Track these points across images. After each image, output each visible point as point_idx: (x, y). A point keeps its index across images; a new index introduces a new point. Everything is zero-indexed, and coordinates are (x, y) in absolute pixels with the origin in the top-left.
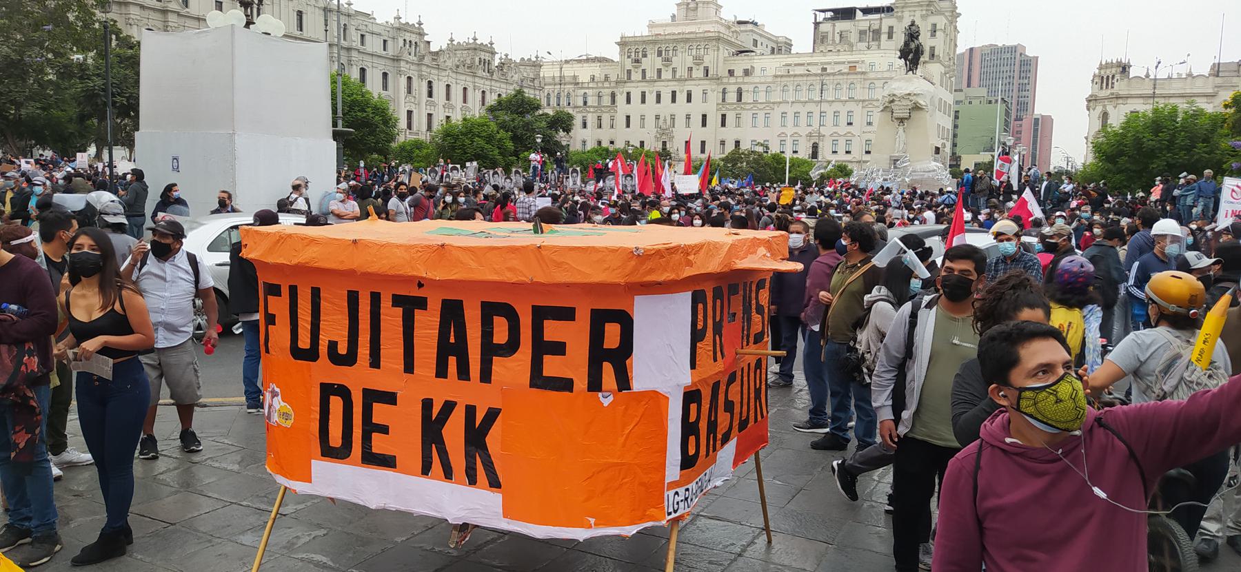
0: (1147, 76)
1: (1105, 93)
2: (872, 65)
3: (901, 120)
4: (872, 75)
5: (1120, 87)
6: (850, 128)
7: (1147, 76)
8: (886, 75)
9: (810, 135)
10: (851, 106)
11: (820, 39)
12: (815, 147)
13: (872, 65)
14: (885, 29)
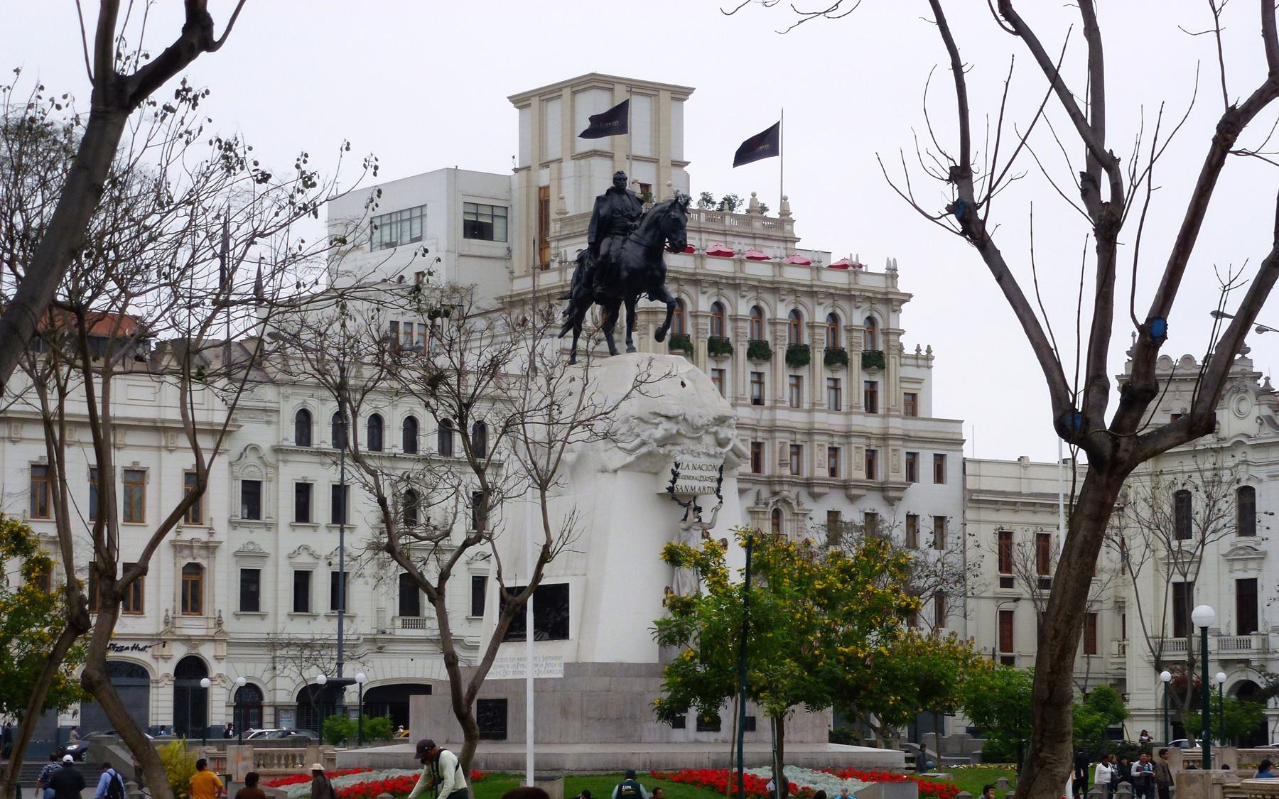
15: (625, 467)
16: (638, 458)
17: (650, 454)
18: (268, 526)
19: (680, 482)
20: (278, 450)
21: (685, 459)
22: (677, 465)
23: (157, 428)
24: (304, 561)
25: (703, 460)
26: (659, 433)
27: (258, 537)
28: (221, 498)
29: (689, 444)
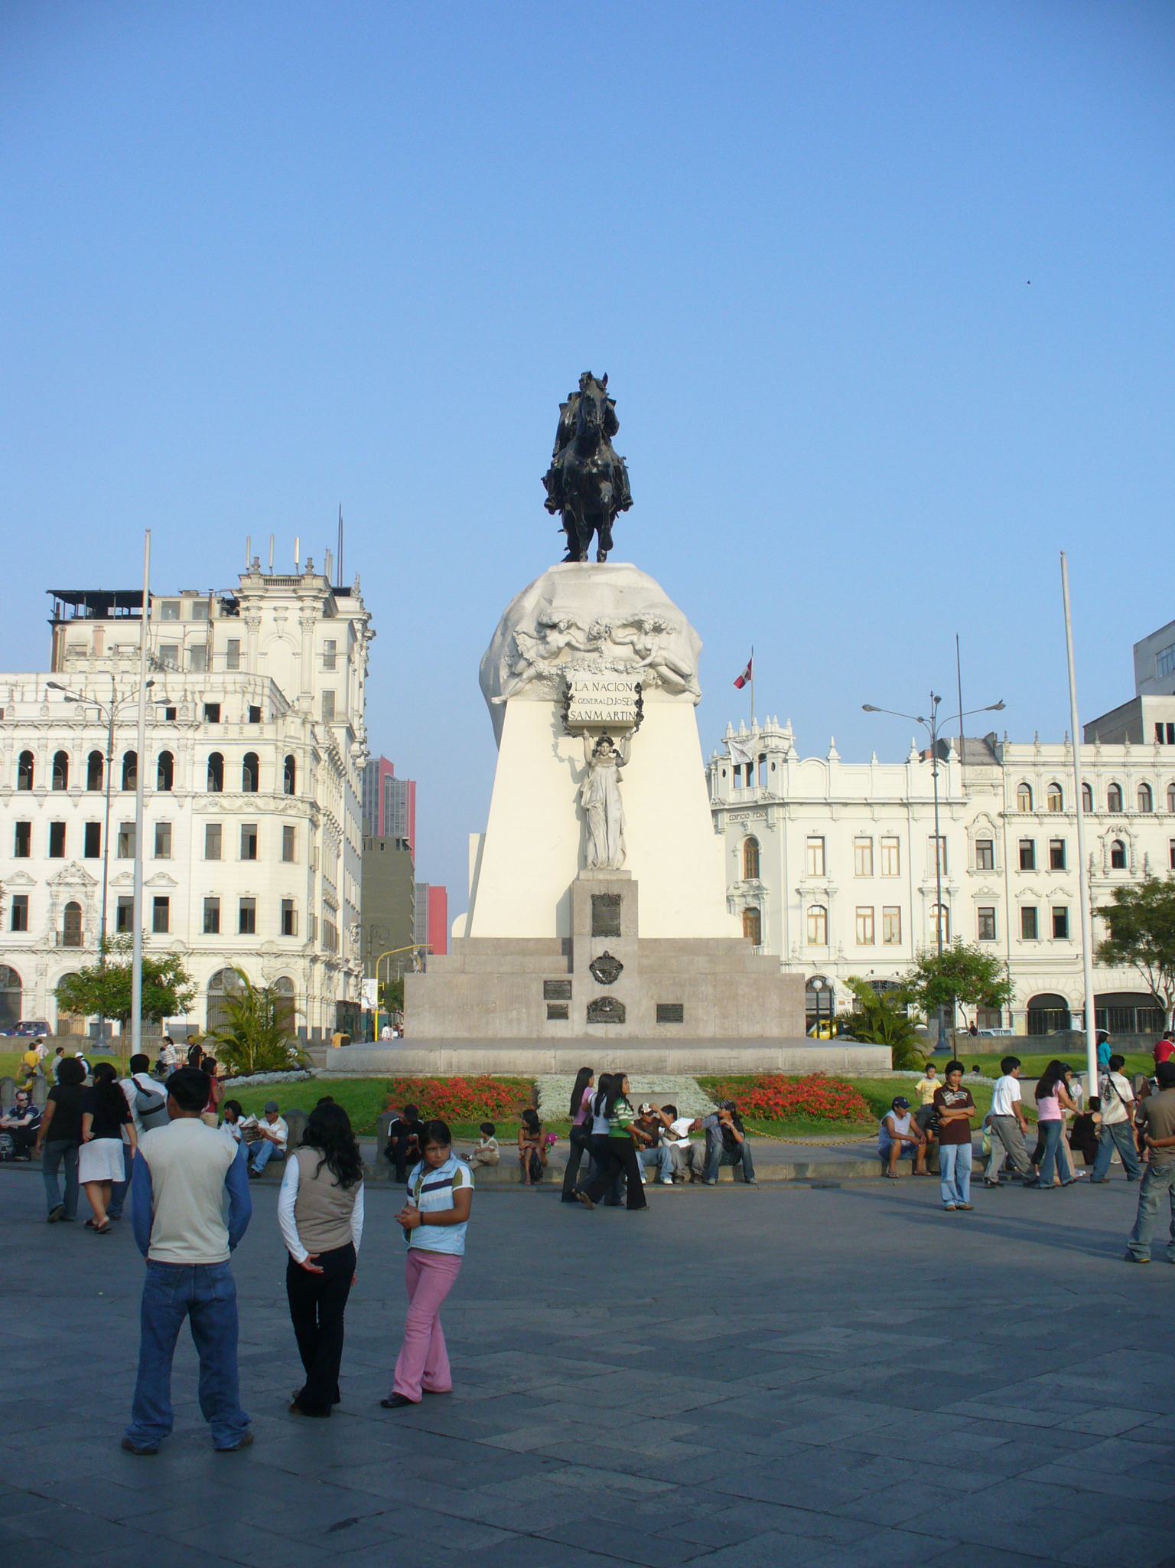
3: (607, 736)
6: (161, 865)
9: (60, 881)
12: (73, 910)
14: (220, 646)
18: (999, 874)
19: (574, 707)
20: (1002, 815)
22: (569, 687)
24: (1029, 901)
27: (991, 881)
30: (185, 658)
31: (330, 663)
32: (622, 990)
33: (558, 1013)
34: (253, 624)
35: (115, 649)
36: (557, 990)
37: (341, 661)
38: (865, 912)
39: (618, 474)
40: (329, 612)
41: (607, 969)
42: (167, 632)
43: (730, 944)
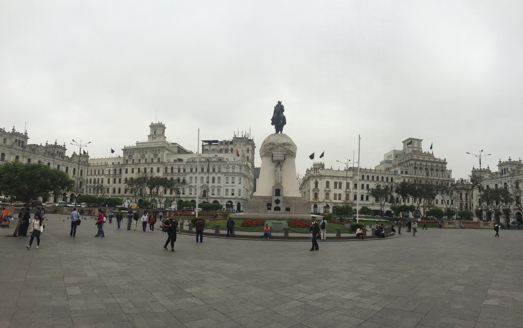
0: (332, 169)
1: (315, 174)
2: (227, 159)
4: (228, 163)
5: (322, 172)
6: (219, 184)
7: (332, 169)
8: (234, 163)
9: (202, 187)
10: (219, 175)
11: (204, 151)
12: (204, 192)
13: (227, 159)
14: (230, 149)
15: (264, 156)
16: (266, 153)
17: (268, 152)
19: (274, 158)
21: (275, 153)
23: (343, 177)
24: (362, 194)
25: (280, 153)
26: (268, 148)
28: (351, 186)
29: (276, 150)
30: (224, 151)
31: (248, 152)
32: (280, 205)
33: (269, 209)
34: (235, 145)
35: (213, 150)
36: (269, 205)
37: (250, 152)
38: (335, 195)
39: (284, 118)
40: (248, 144)
41: (277, 202)
42: (222, 147)
43: (298, 198)
